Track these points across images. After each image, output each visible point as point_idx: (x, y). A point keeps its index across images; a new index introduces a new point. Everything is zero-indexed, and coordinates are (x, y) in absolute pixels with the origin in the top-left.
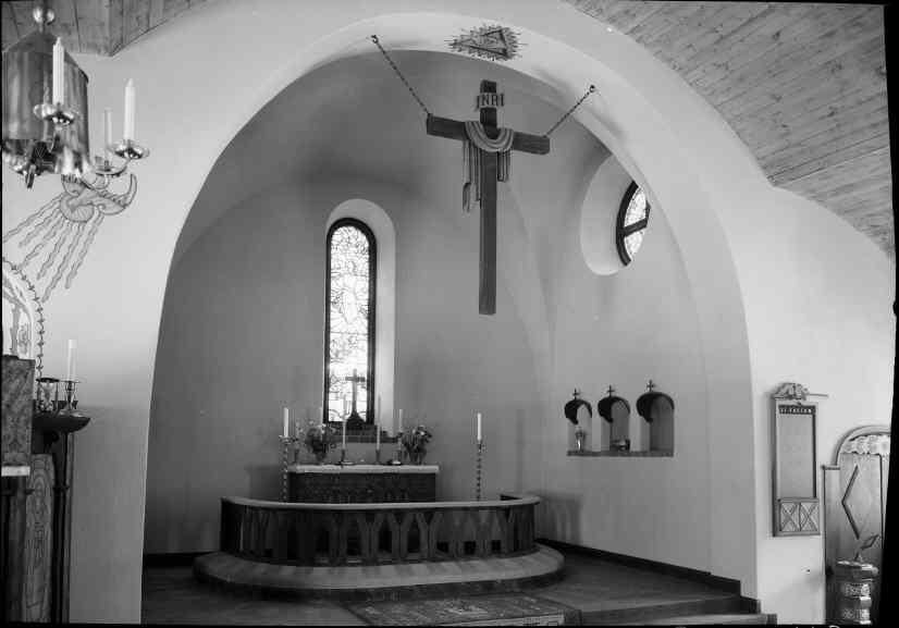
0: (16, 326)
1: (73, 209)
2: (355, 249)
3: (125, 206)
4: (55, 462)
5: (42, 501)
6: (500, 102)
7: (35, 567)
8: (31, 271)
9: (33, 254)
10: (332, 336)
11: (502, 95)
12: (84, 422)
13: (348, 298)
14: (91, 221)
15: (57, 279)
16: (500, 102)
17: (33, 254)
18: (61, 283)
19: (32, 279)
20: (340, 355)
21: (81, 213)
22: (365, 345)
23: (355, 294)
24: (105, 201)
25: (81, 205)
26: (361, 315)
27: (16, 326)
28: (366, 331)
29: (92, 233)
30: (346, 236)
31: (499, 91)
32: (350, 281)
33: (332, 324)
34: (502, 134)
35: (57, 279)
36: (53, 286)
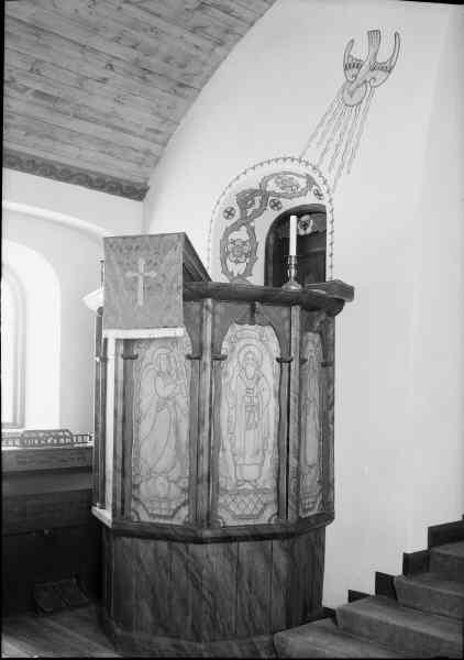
1: (351, 94)
8: (323, 168)
9: (326, 150)
14: (364, 101)
17: (326, 150)
18: (345, 170)
21: (356, 98)
25: (358, 87)
29: (367, 110)
36: (339, 175)
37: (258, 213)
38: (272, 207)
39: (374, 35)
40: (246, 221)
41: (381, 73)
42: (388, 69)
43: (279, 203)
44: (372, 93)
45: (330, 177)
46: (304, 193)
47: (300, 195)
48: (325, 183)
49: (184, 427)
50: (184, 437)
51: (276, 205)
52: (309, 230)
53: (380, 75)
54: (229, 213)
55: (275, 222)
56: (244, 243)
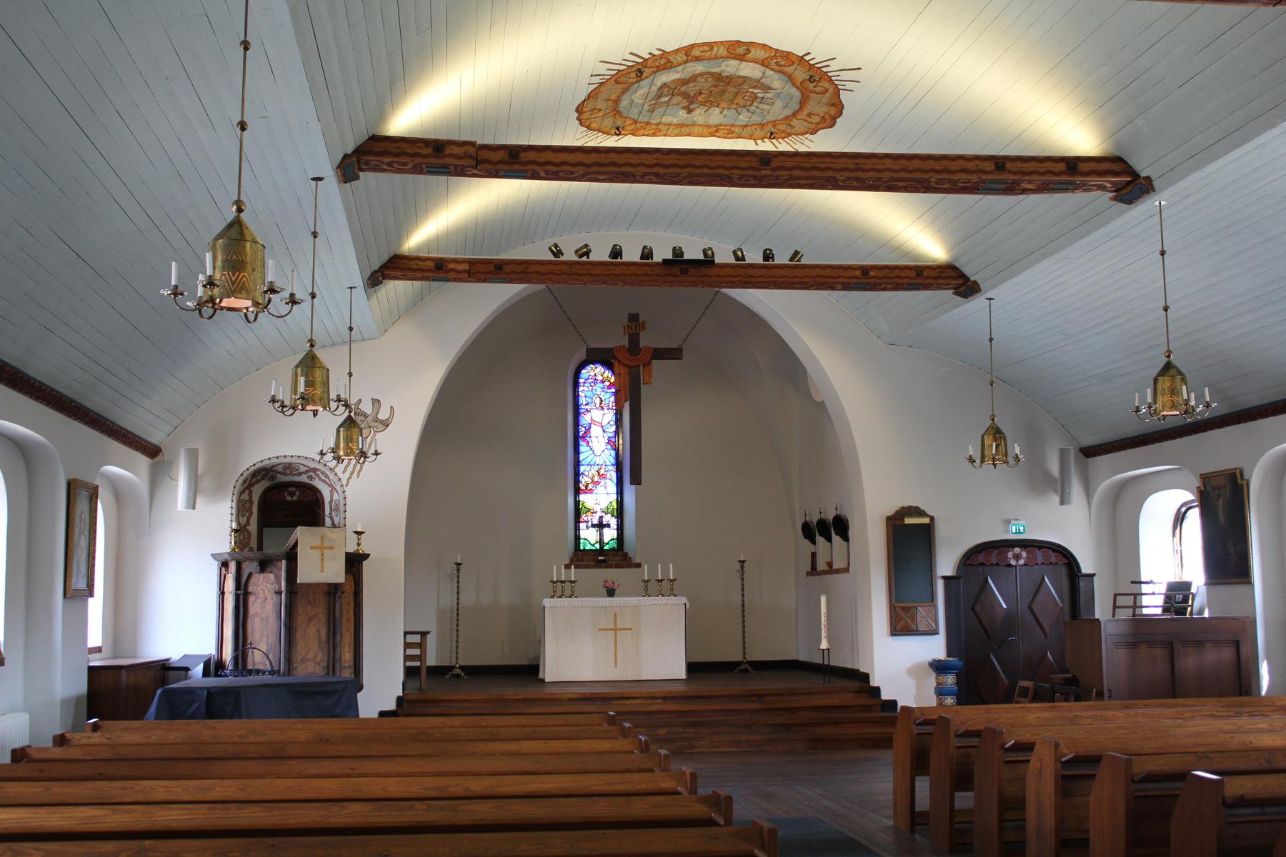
0: (332, 500)
2: (601, 385)
3: (387, 426)
4: (354, 579)
5: (349, 599)
6: (641, 328)
7: (347, 632)
10: (582, 469)
11: (643, 323)
12: (366, 556)
13: (595, 431)
15: (352, 473)
16: (641, 328)
19: (340, 474)
20: (590, 487)
22: (614, 475)
23: (602, 427)
24: (376, 424)
26: (609, 447)
27: (332, 500)
28: (613, 461)
30: (592, 374)
31: (641, 320)
32: (596, 415)
33: (582, 457)
34: (643, 352)
35: (352, 473)
36: (349, 478)
37: (258, 482)
38: (269, 479)
39: (376, 402)
40: (251, 485)
41: (381, 425)
42: (386, 424)
43: (276, 477)
44: (375, 435)
45: (344, 478)
46: (300, 474)
47: (295, 475)
48: (340, 480)
49: (324, 632)
50: (324, 638)
51: (273, 478)
52: (295, 498)
53: (381, 427)
54: (245, 482)
55: (264, 491)
56: (246, 502)
